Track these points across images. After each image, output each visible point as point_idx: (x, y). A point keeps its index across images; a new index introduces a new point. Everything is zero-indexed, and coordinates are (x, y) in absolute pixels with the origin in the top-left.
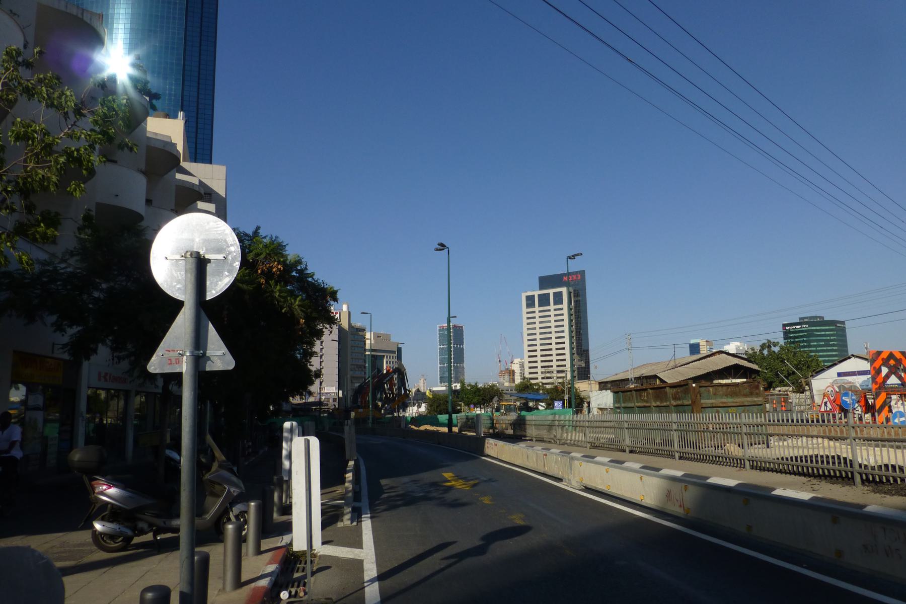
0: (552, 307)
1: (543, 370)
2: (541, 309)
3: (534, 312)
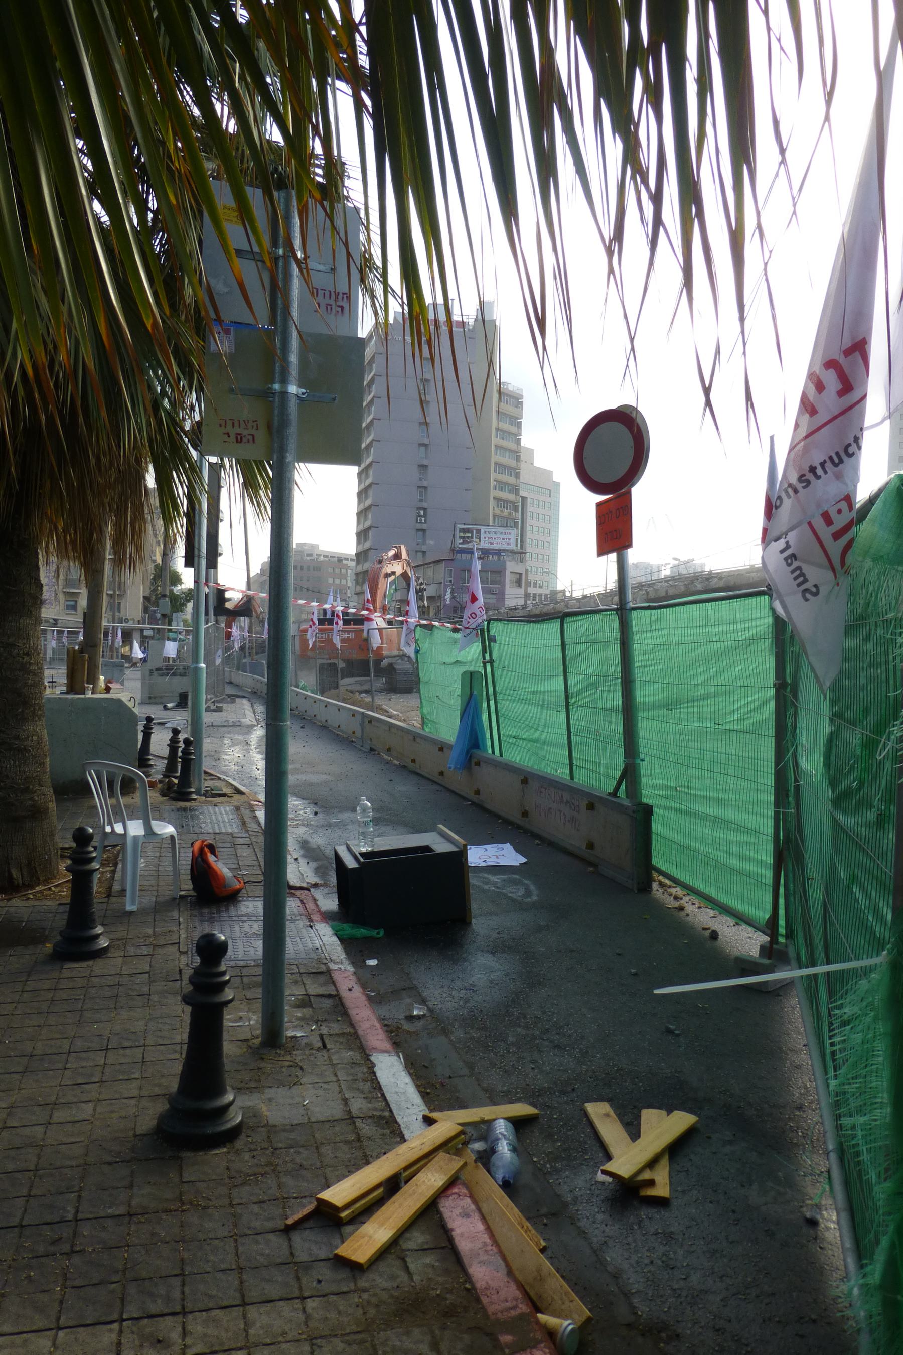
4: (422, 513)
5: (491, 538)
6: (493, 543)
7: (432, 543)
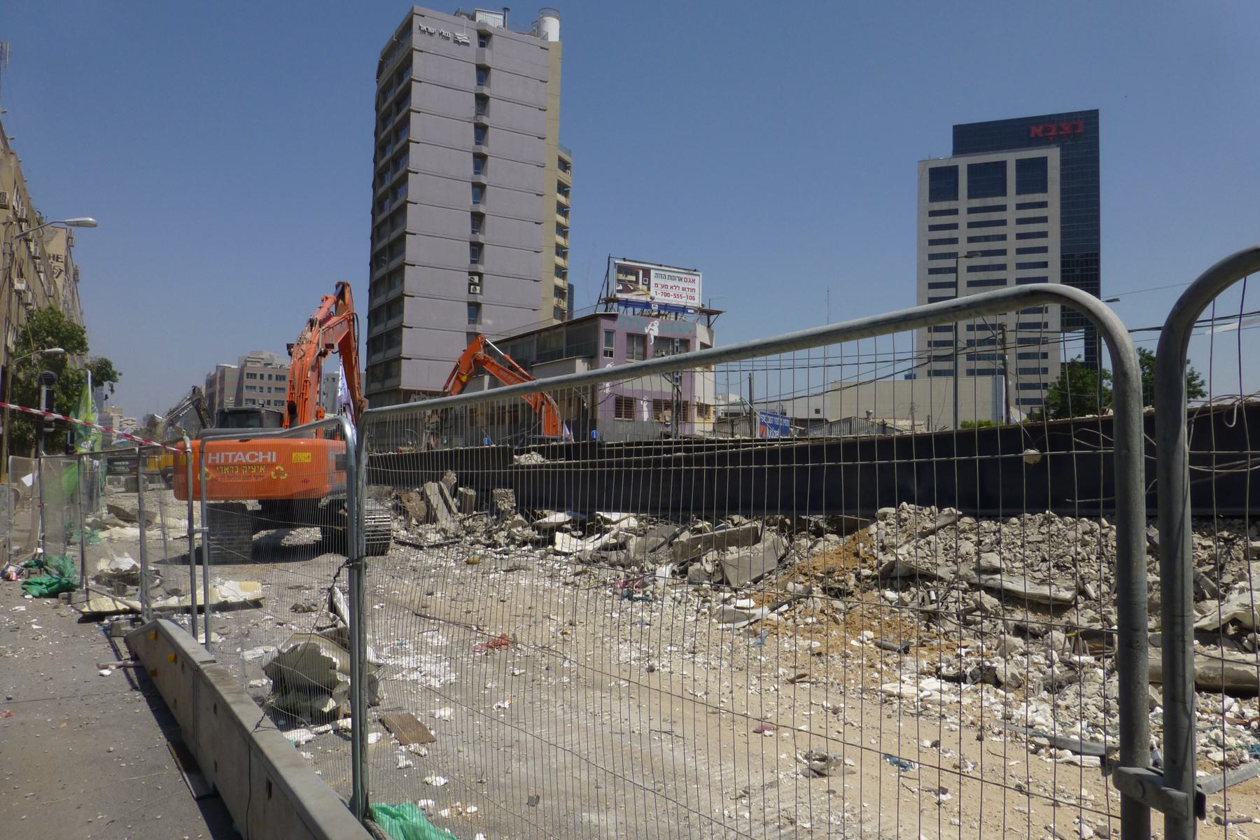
0: (1012, 198)
2: (976, 203)
3: (955, 212)
4: (476, 279)
5: (666, 286)
6: (667, 295)
7: (489, 322)
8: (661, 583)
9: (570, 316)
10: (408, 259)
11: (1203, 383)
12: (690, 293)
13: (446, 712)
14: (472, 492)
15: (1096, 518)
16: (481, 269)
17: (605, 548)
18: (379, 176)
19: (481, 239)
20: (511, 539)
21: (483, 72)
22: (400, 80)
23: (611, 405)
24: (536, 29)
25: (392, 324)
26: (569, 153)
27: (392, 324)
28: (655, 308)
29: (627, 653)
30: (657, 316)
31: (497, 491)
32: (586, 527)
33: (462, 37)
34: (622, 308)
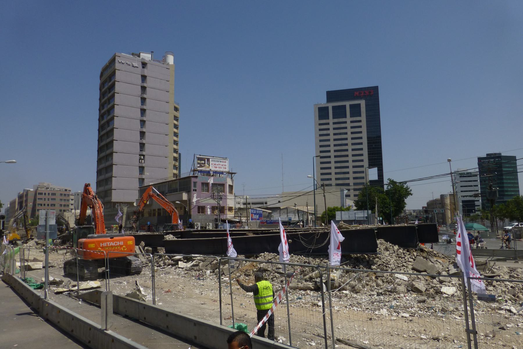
0: (348, 119)
1: (347, 181)
2: (336, 120)
3: (328, 124)
4: (142, 157)
6: (216, 167)
7: (148, 174)
8: (207, 275)
9: (180, 176)
10: (115, 150)
11: (411, 190)
12: (224, 167)
13: (160, 304)
14: (150, 249)
15: (301, 255)
16: (144, 153)
17: (194, 266)
18: (101, 117)
19: (144, 141)
20: (165, 264)
21: (144, 78)
22: (110, 81)
23: (196, 209)
24: (164, 60)
25: (108, 175)
26: (178, 104)
27: (108, 175)
28: (212, 173)
29: (197, 291)
30: (213, 176)
31: (159, 248)
32: (188, 260)
33: (135, 64)
34: (199, 173)
